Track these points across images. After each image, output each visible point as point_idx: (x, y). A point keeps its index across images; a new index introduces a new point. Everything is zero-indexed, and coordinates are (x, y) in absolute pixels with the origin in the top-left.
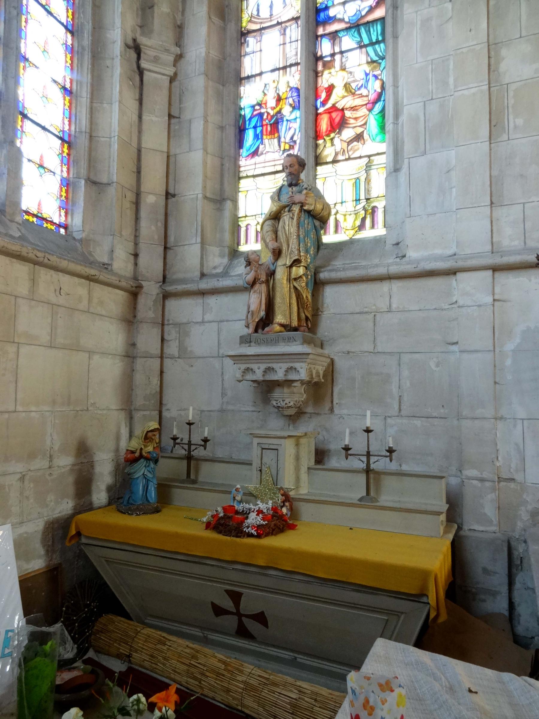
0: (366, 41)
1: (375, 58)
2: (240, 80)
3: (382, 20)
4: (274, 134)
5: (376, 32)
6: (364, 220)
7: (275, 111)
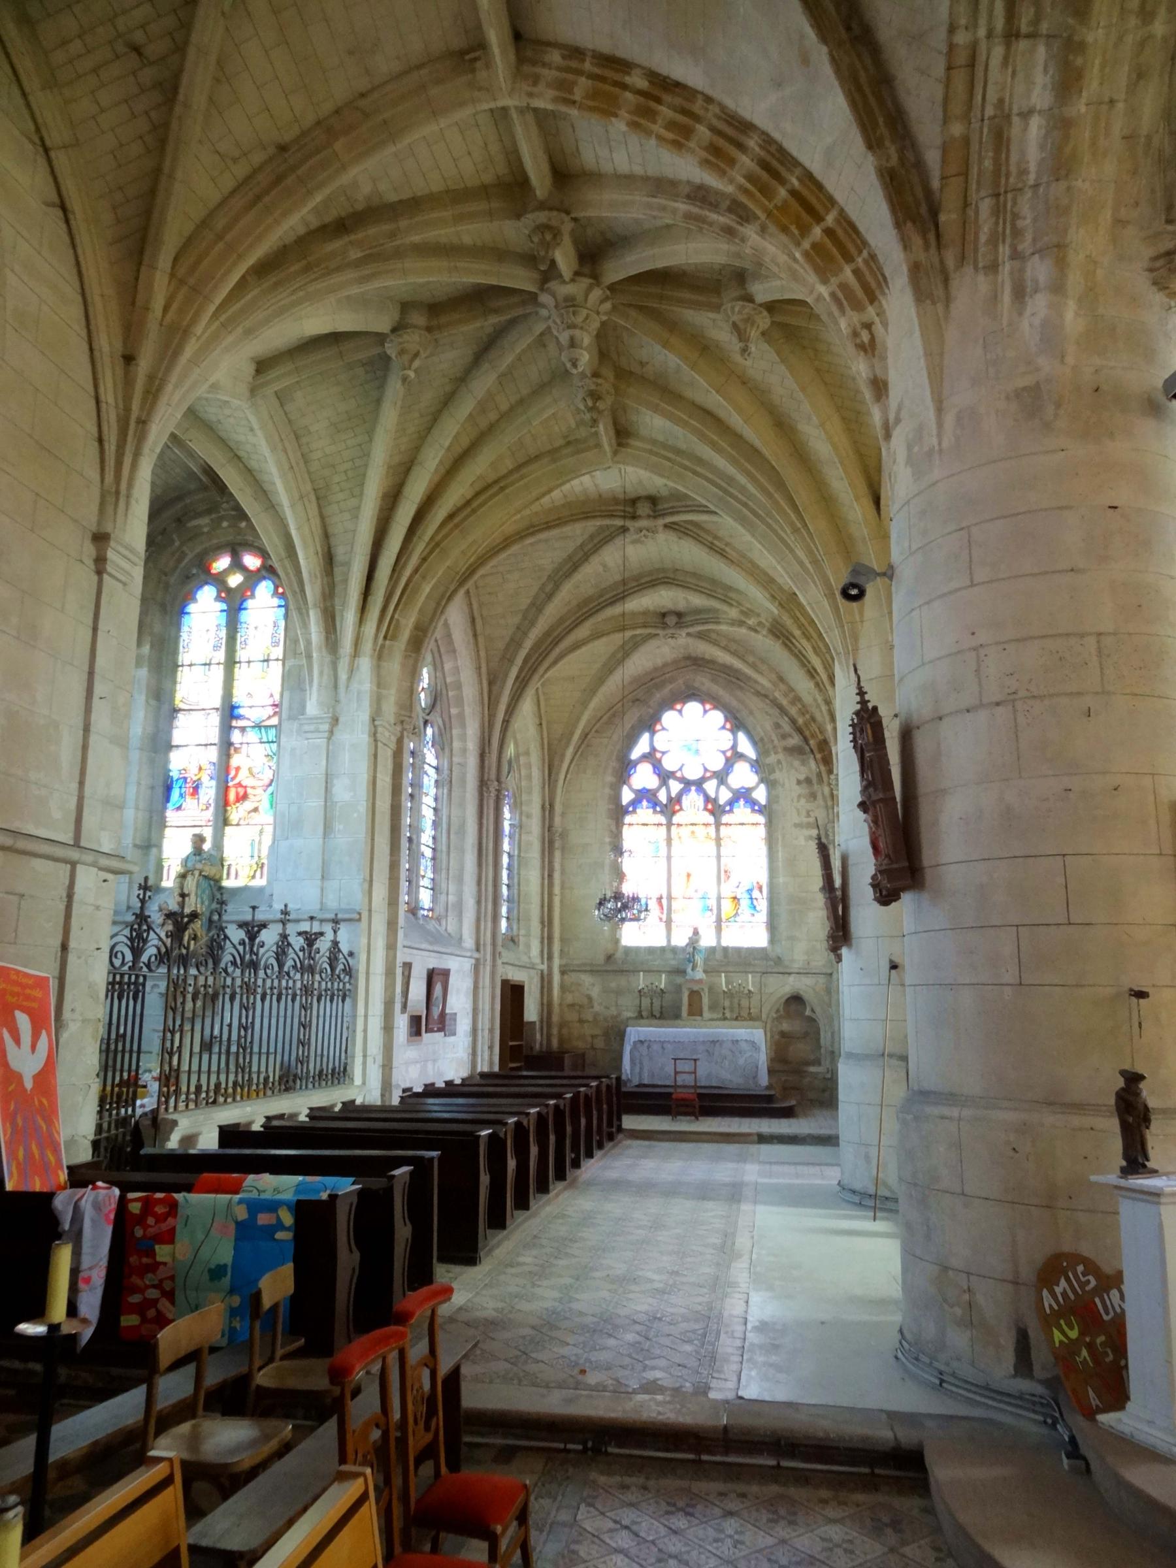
2: (170, 747)
3: (275, 726)
5: (272, 733)
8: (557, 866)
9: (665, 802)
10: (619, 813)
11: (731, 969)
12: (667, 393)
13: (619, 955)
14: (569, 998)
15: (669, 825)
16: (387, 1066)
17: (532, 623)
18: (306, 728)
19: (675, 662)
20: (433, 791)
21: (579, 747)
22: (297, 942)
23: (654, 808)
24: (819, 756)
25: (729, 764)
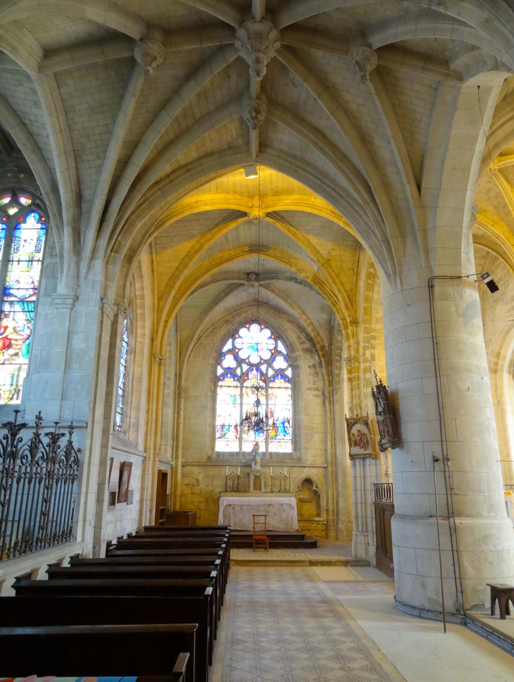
1: (30, 319)
3: (34, 302)
5: (31, 307)
6: (13, 395)
8: (182, 407)
9: (239, 375)
10: (216, 380)
11: (274, 464)
12: (296, 116)
13: (214, 456)
14: (186, 481)
15: (242, 387)
16: (98, 528)
17: (186, 266)
18: (57, 301)
19: (247, 302)
20: (125, 356)
21: (196, 344)
22: (46, 440)
23: (234, 378)
24: (321, 353)
25: (273, 358)
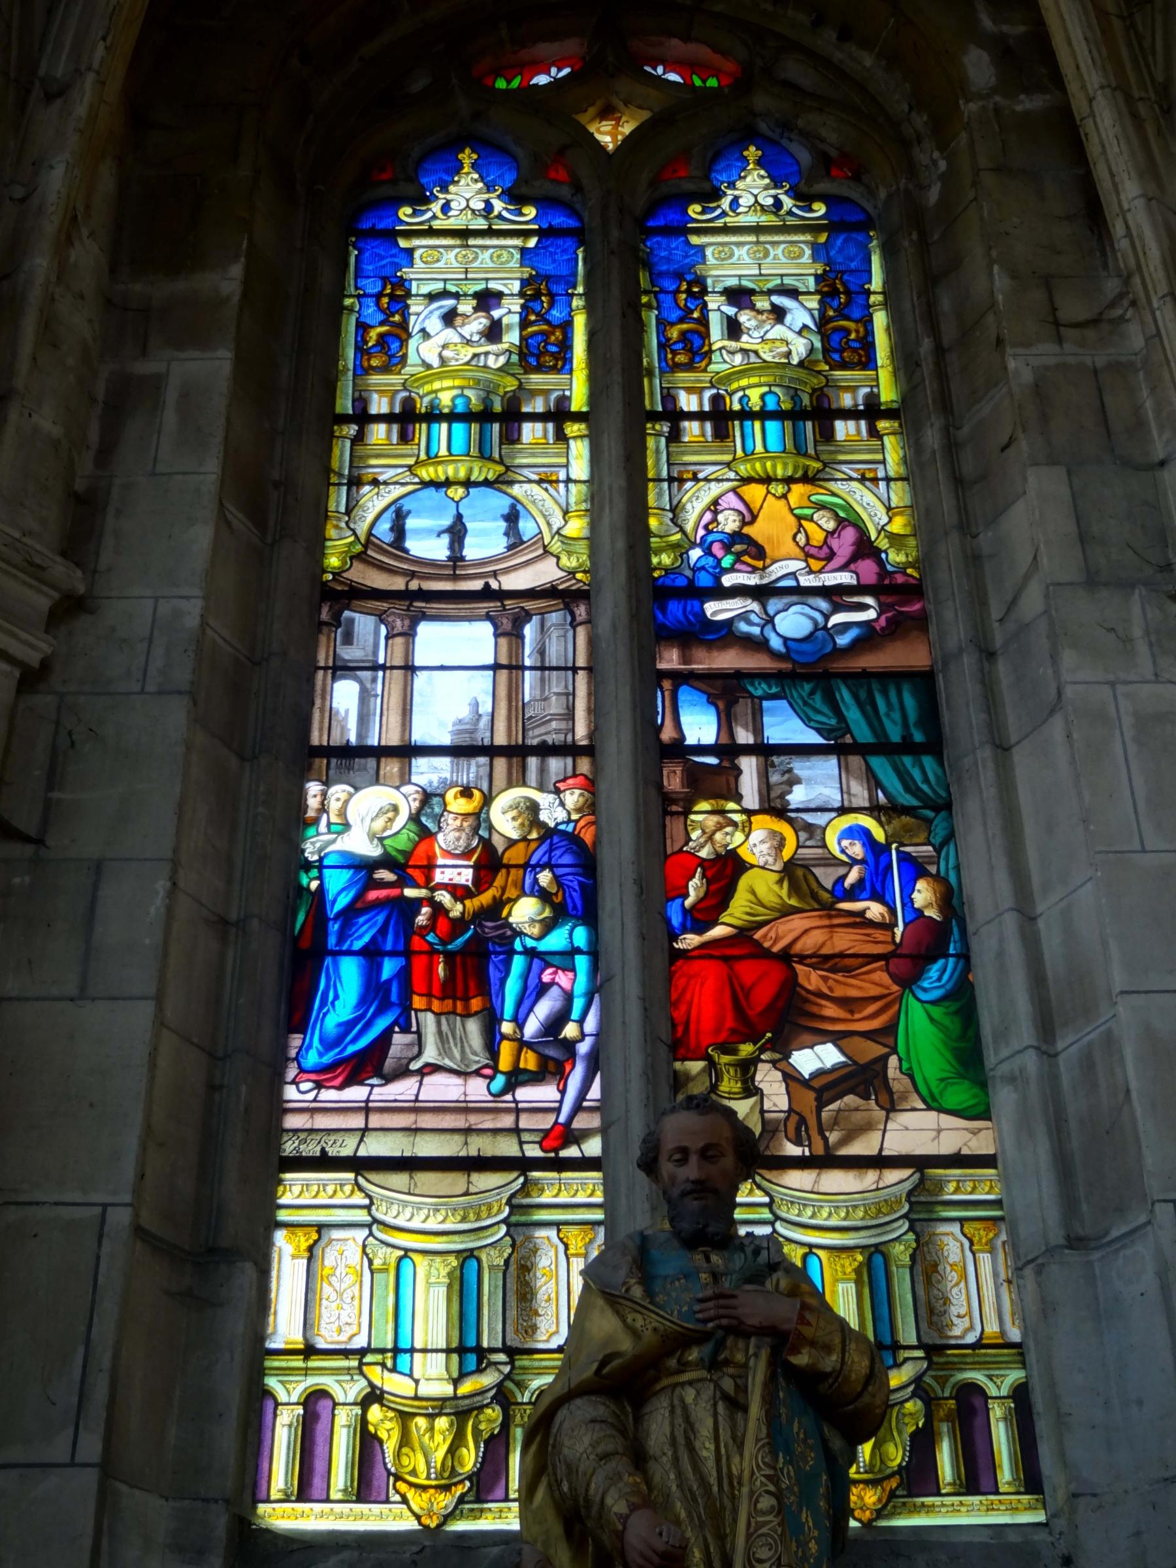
0: (862, 733)
1: (908, 800)
3: (924, 682)
4: (466, 999)
5: (898, 714)
7: (472, 904)
